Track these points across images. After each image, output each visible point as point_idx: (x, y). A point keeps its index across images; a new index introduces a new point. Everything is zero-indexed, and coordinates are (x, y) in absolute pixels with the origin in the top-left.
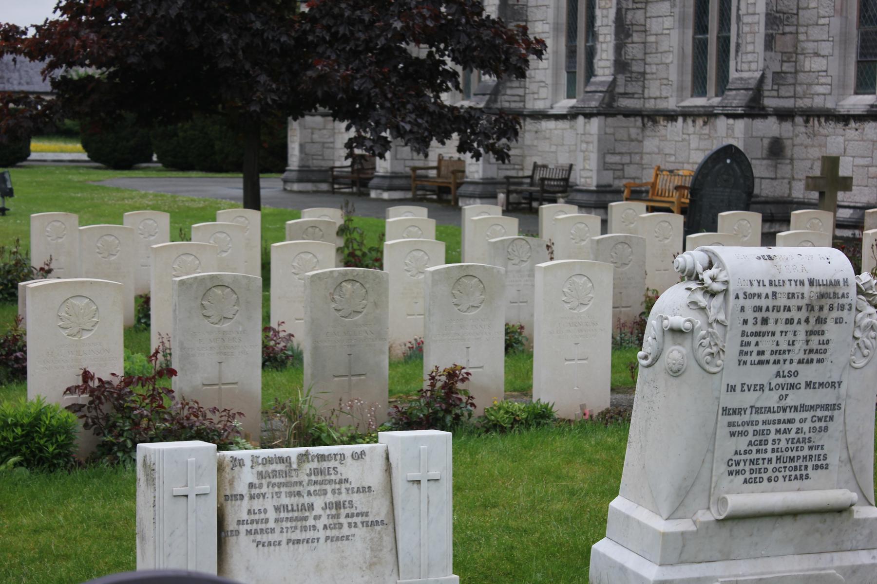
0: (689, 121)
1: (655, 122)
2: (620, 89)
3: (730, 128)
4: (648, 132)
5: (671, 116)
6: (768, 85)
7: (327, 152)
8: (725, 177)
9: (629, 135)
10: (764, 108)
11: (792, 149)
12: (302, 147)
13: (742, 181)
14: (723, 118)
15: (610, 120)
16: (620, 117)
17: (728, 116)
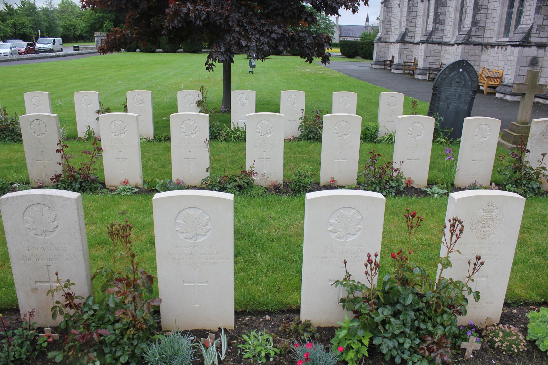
0: (500, 48)
1: (487, 48)
2: (473, 34)
3: (512, 52)
4: (483, 52)
5: (493, 46)
6: (534, 31)
7: (386, 55)
8: (458, 80)
9: (475, 53)
10: (530, 42)
11: (542, 63)
12: (377, 53)
13: (470, 83)
14: (510, 47)
15: (467, 46)
16: (472, 45)
17: (512, 46)
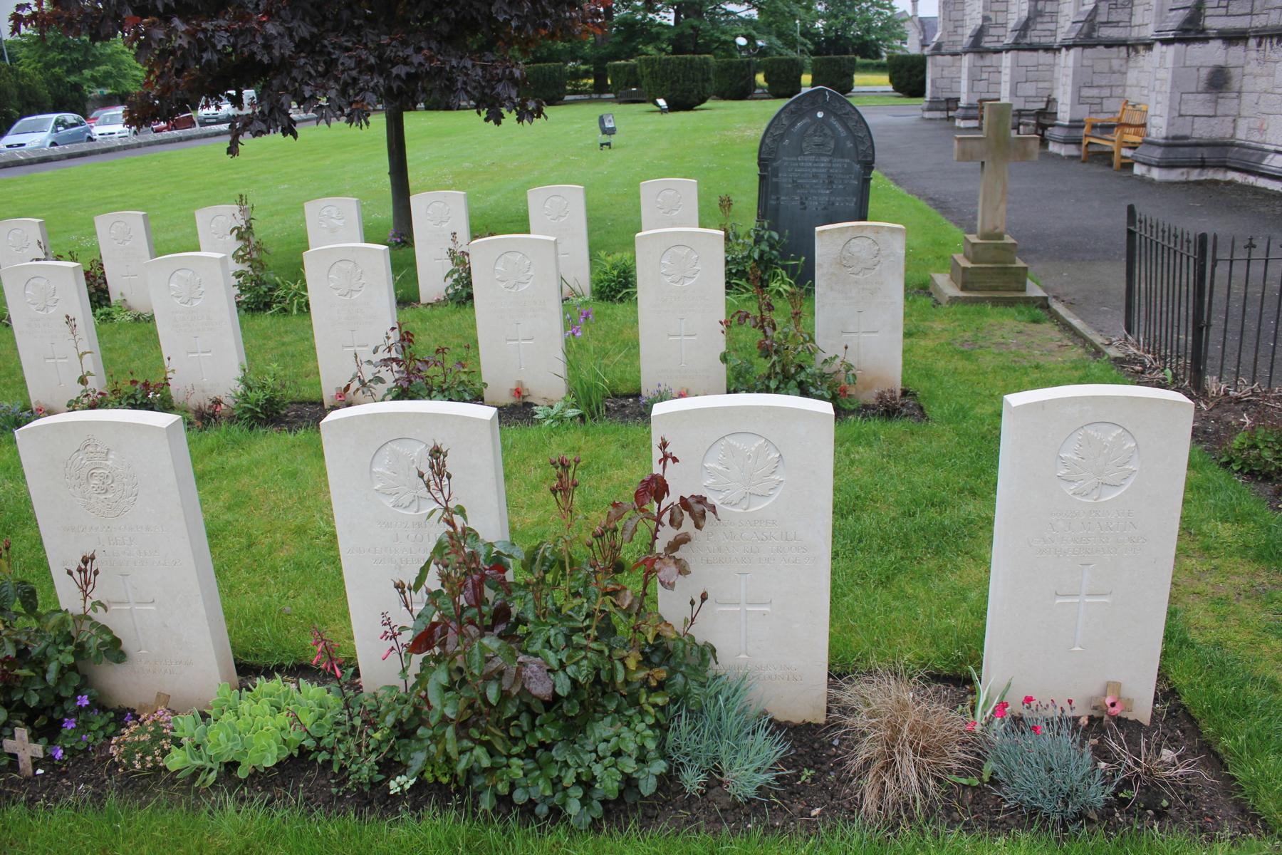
1: (1137, 52)
2: (1102, 18)
3: (1163, 57)
4: (1131, 64)
8: (817, 139)
9: (1110, 68)
10: (1204, 30)
11: (1241, 80)
12: (932, 81)
13: (849, 145)
14: (1157, 47)
15: (1088, 51)
16: (1101, 48)
